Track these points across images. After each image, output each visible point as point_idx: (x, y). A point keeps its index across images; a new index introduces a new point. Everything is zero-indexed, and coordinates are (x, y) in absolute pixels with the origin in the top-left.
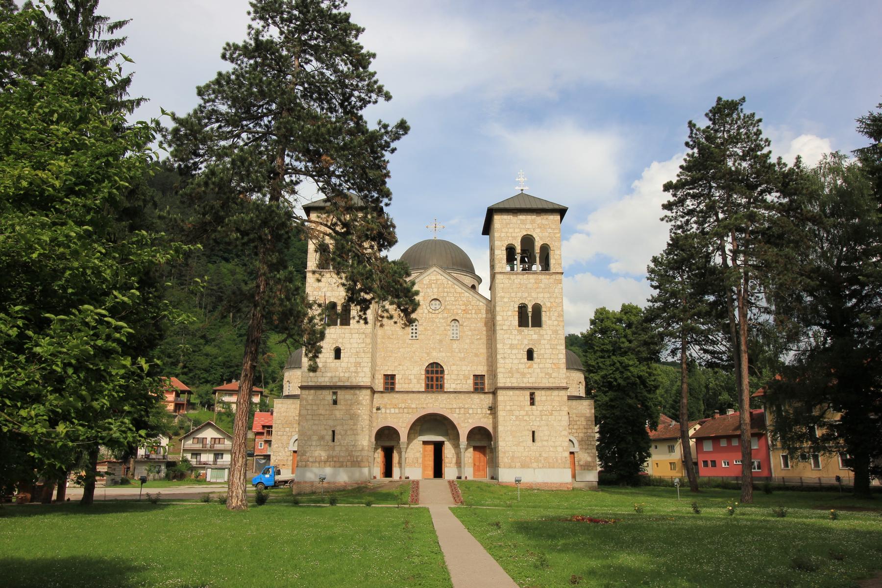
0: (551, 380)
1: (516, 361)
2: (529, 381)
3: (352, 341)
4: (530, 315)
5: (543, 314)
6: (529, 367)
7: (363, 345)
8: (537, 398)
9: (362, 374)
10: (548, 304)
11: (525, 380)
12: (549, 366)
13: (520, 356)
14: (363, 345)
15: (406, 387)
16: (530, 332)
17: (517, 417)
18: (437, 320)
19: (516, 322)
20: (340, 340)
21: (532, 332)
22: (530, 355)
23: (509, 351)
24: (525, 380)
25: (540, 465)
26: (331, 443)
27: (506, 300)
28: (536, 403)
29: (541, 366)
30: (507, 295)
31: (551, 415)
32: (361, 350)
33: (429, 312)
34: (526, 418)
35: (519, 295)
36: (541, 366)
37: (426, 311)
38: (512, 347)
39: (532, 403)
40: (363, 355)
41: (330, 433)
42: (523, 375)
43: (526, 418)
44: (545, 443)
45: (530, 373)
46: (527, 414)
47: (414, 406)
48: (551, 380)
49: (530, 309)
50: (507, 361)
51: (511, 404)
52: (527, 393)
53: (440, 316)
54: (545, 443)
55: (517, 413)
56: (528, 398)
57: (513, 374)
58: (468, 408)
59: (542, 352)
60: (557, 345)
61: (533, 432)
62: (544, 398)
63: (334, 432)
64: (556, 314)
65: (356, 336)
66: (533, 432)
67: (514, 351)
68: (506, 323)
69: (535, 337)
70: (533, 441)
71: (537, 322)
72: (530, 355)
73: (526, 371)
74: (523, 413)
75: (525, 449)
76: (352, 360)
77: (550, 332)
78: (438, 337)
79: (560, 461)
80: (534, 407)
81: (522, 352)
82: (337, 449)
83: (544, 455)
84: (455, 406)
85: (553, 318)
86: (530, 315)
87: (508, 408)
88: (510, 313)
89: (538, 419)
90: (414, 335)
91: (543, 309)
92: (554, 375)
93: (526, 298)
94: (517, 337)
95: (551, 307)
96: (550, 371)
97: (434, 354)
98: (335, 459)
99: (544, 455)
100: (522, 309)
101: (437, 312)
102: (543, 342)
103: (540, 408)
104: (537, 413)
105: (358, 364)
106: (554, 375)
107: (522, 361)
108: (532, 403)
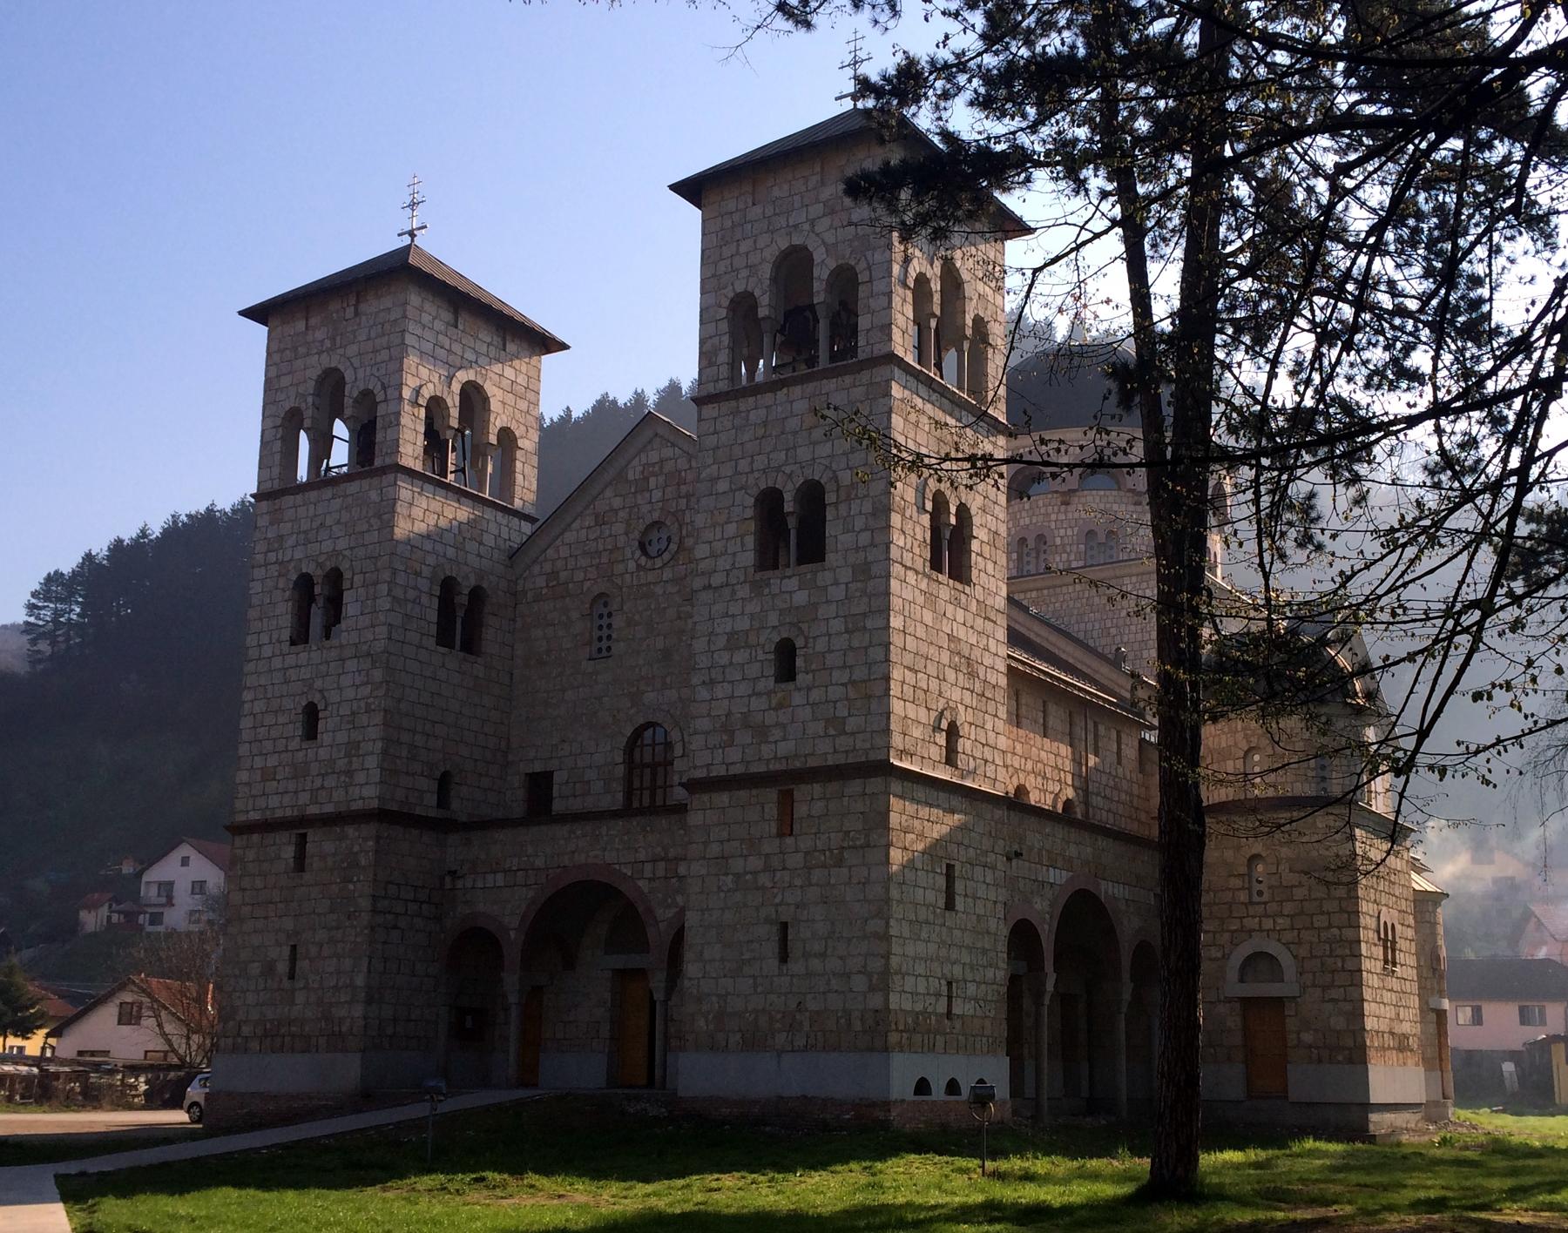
0: (843, 742)
1: (742, 689)
2: (780, 751)
3: (346, 681)
4: (792, 523)
5: (830, 514)
6: (780, 706)
7: (366, 690)
8: (801, 810)
9: (360, 777)
10: (846, 478)
11: (766, 751)
12: (836, 692)
13: (753, 670)
14: (366, 690)
15: (576, 805)
16: (791, 587)
17: (738, 876)
18: (659, 590)
19: (748, 558)
20: (318, 684)
21: (792, 583)
22: (786, 661)
23: (724, 658)
24: (766, 751)
25: (800, 1042)
26: (286, 984)
27: (723, 486)
28: (796, 827)
29: (816, 695)
30: (727, 470)
31: (840, 863)
32: (362, 704)
33: (639, 567)
34: (764, 880)
35: (760, 462)
36: (816, 695)
37: (632, 565)
38: (734, 641)
39: (787, 825)
40: (364, 719)
41: (286, 951)
42: (761, 732)
43: (764, 880)
44: (816, 964)
45: (783, 726)
46: (767, 868)
47: (539, 862)
48: (843, 742)
49: (788, 507)
50: (720, 691)
51: (725, 835)
52: (771, 795)
53: (667, 574)
54: (816, 964)
55: (737, 865)
56: (772, 810)
57: (732, 733)
58: (678, 859)
59: (821, 645)
60: (864, 615)
61: (784, 927)
62: (818, 808)
63: (294, 947)
64: (867, 507)
65: (351, 665)
66: (784, 927)
67: (740, 656)
68: (724, 563)
69: (801, 598)
70: (784, 957)
71: (813, 550)
72: (786, 661)
73: (770, 718)
74: (755, 863)
75: (755, 986)
76: (342, 737)
77: (845, 575)
78: (660, 643)
79: (857, 1025)
80: (789, 841)
81: (761, 657)
82: (300, 998)
83: (812, 1005)
84: (642, 856)
85: (859, 523)
86: (792, 523)
87: (715, 849)
88: (731, 529)
89: (798, 882)
90: (604, 644)
91: (830, 498)
92: (852, 724)
93: (778, 469)
94: (752, 607)
95: (853, 485)
96: (842, 711)
97: (650, 697)
98: (293, 1029)
99: (812, 1005)
100: (769, 501)
101: (658, 562)
102: (823, 611)
103: (806, 843)
104: (796, 860)
105: (353, 748)
106: (852, 724)
107: (762, 685)
108: (787, 825)
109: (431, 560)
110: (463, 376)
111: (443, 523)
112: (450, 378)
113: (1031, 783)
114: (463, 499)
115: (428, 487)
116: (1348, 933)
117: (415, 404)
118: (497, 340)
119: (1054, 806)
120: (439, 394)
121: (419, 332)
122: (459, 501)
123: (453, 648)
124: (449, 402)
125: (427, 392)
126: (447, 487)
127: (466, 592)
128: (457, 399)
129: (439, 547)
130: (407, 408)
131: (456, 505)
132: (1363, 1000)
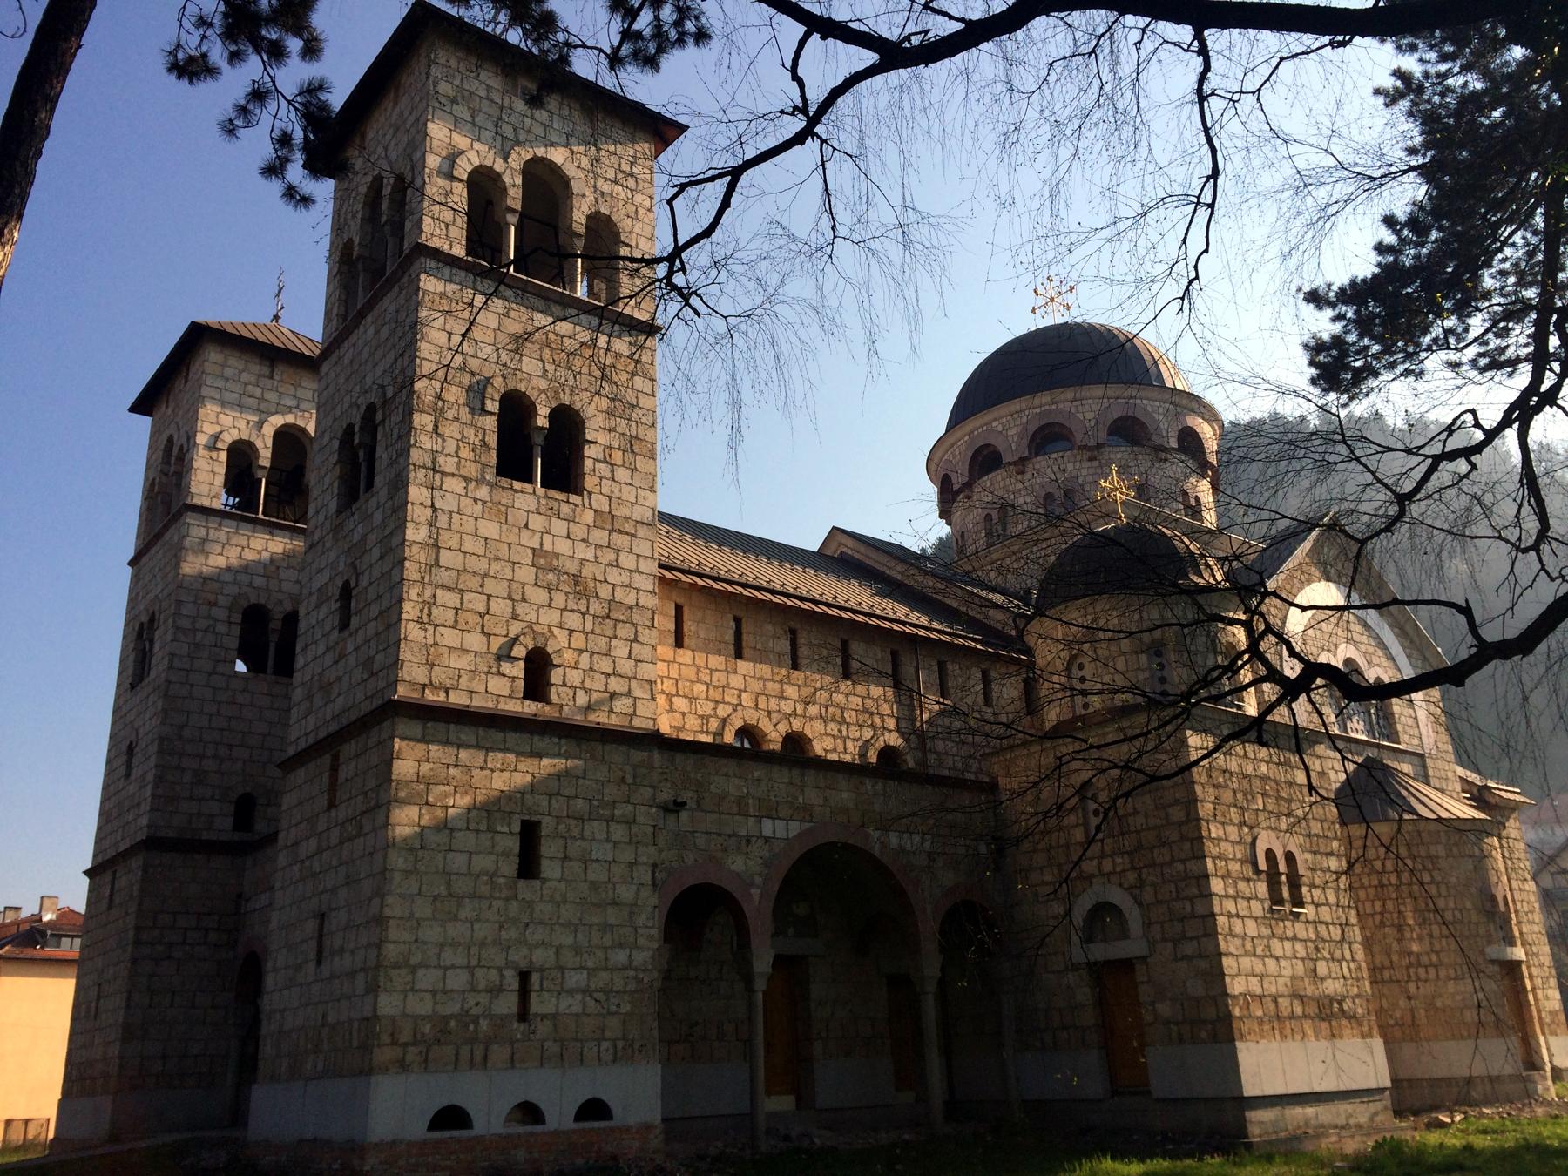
109: (234, 590)
110: (277, 421)
111: (250, 556)
112: (260, 425)
113: (813, 730)
114: (277, 531)
115: (243, 524)
116: (1193, 866)
117: (212, 447)
118: (266, 370)
119: (863, 755)
120: (245, 437)
121: (220, 384)
122: (271, 533)
123: (264, 672)
124: (259, 444)
125: (228, 438)
126: (262, 522)
127: (280, 616)
128: (269, 443)
129: (244, 578)
130: (201, 452)
131: (267, 537)
132: (1220, 954)
